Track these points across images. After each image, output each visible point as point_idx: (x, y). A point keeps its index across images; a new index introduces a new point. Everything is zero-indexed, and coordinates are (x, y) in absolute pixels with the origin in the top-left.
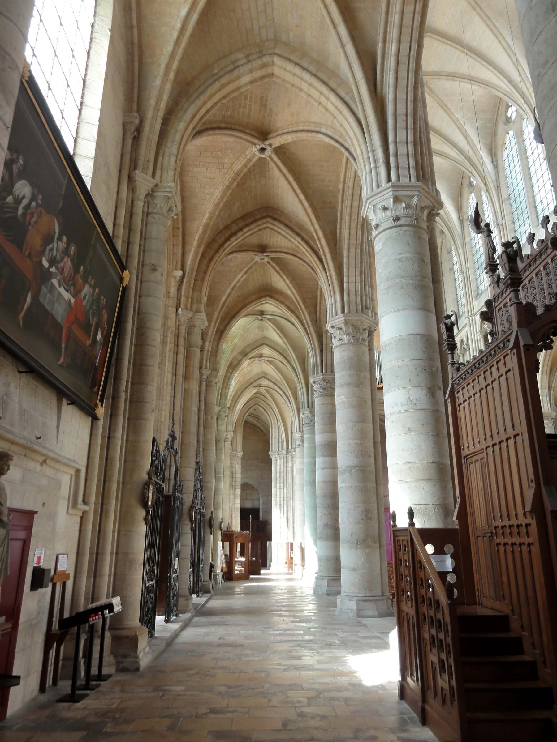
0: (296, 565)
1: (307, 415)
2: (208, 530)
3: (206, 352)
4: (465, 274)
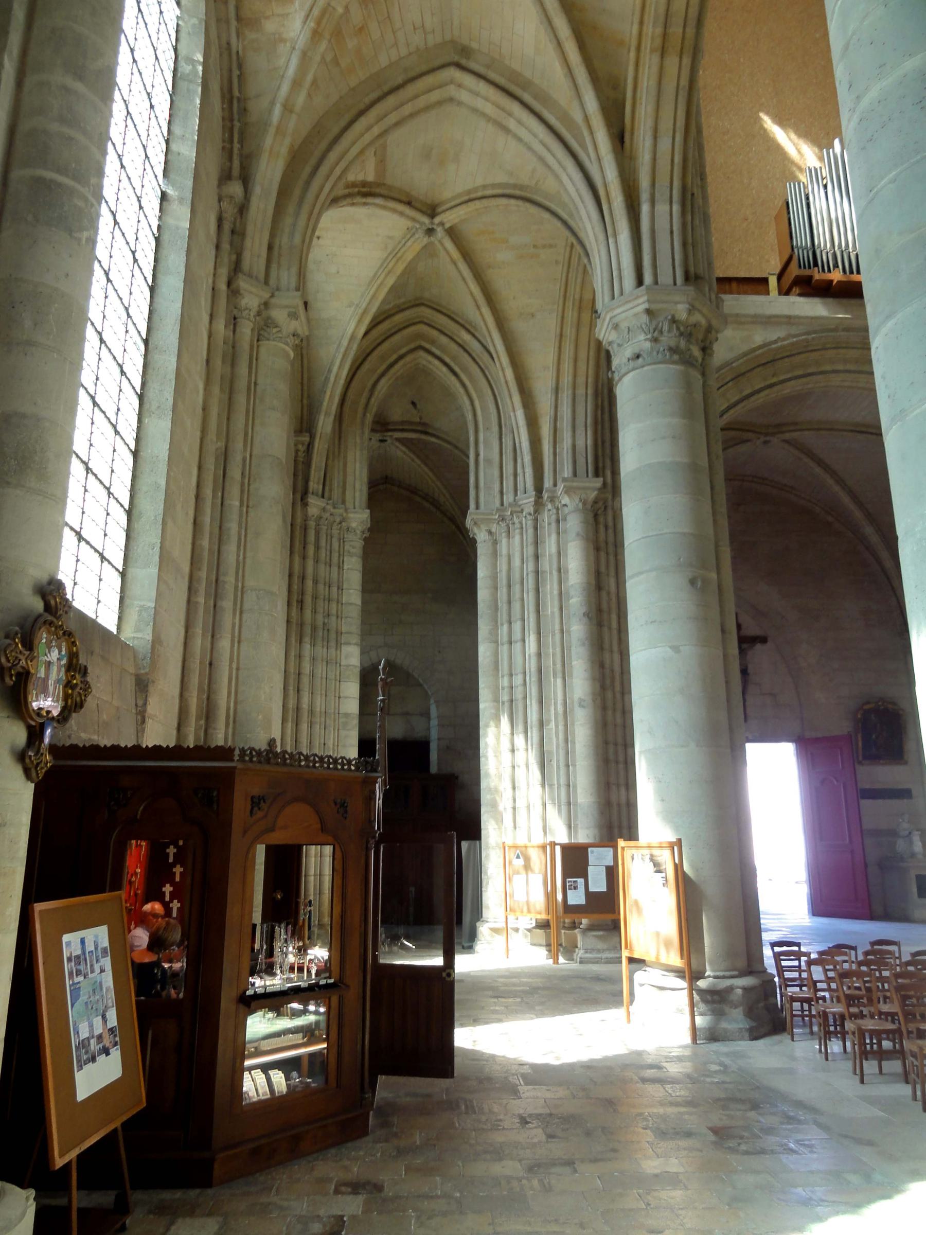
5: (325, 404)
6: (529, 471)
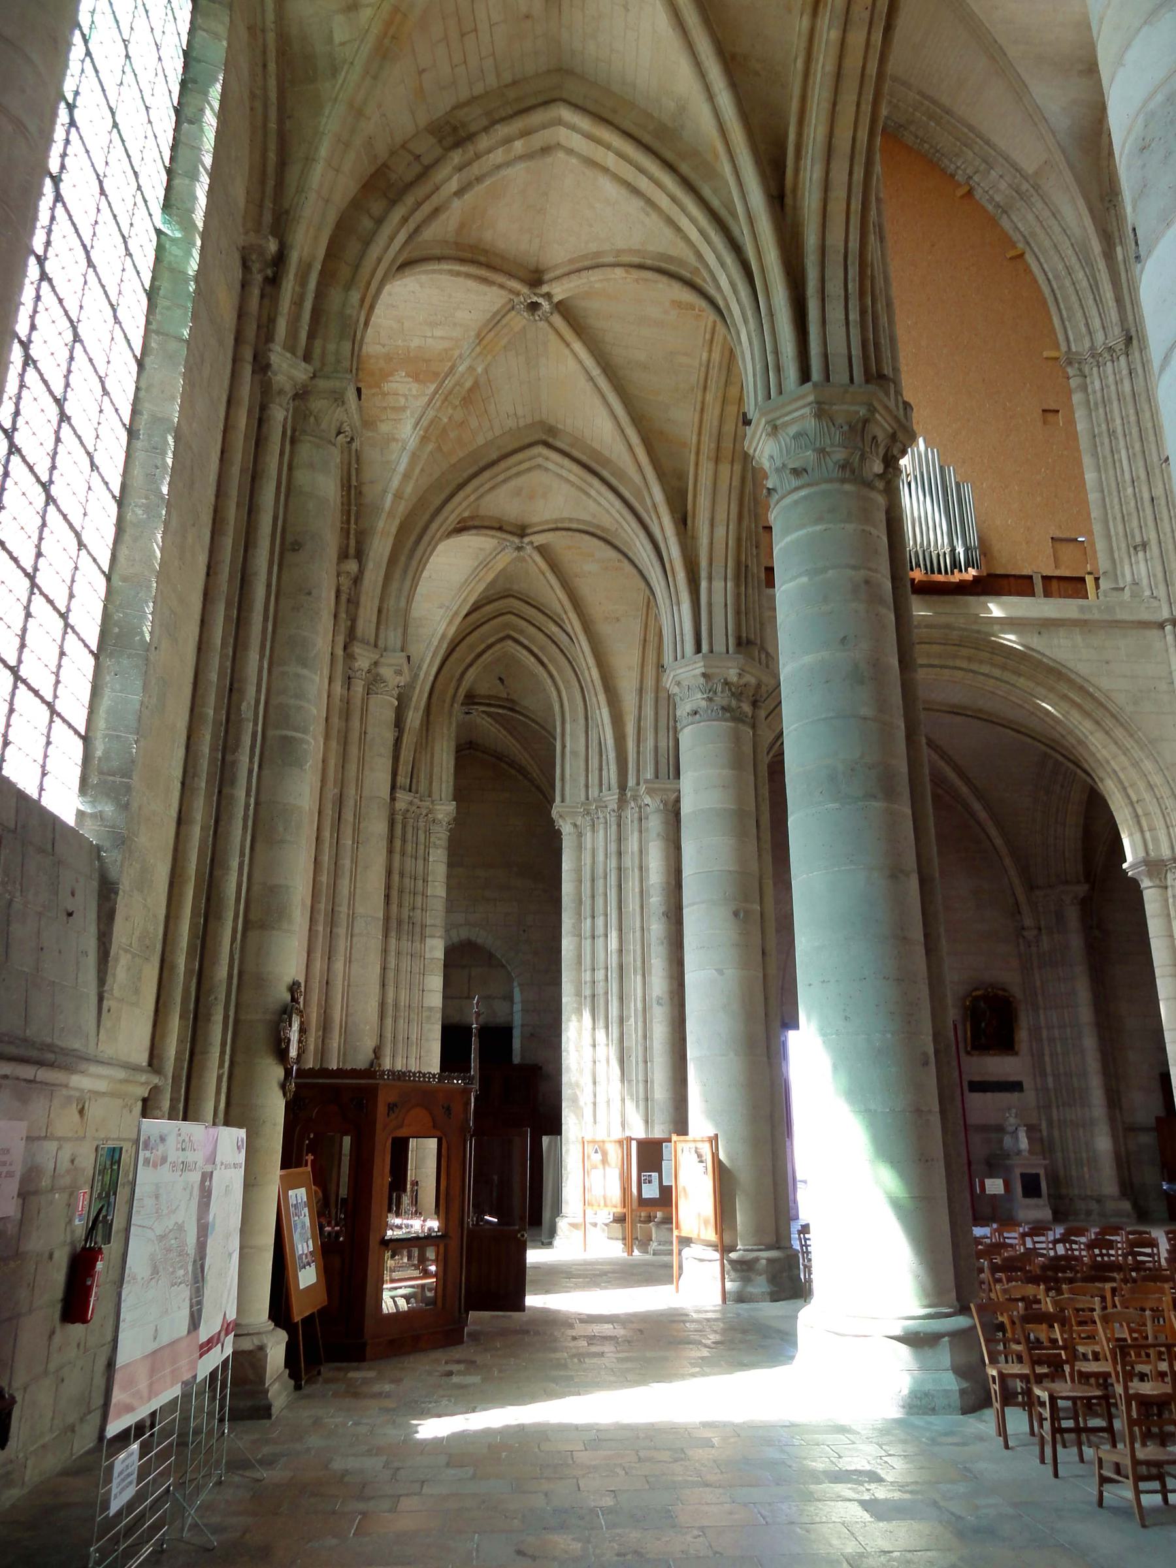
0: (686, 1241)
1: (793, 430)
5: (414, 699)
6: (613, 768)
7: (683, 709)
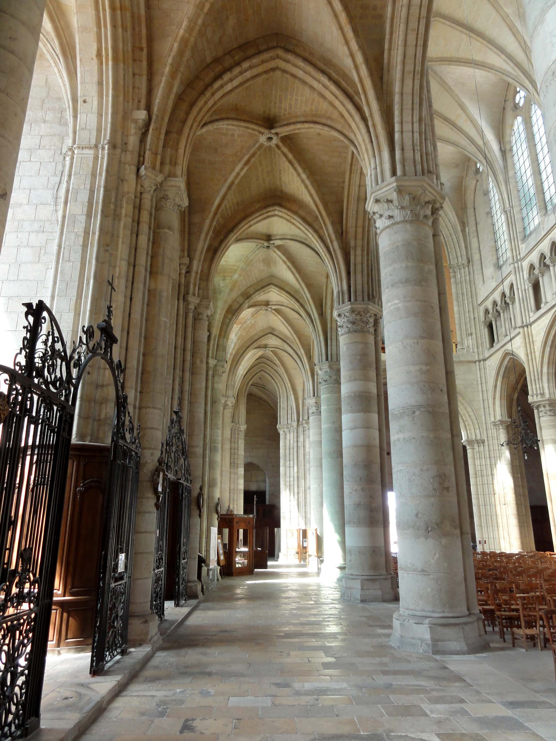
0: (310, 556)
1: (325, 370)
2: (195, 512)
3: (193, 274)
4: (509, 214)
7: (310, 411)
